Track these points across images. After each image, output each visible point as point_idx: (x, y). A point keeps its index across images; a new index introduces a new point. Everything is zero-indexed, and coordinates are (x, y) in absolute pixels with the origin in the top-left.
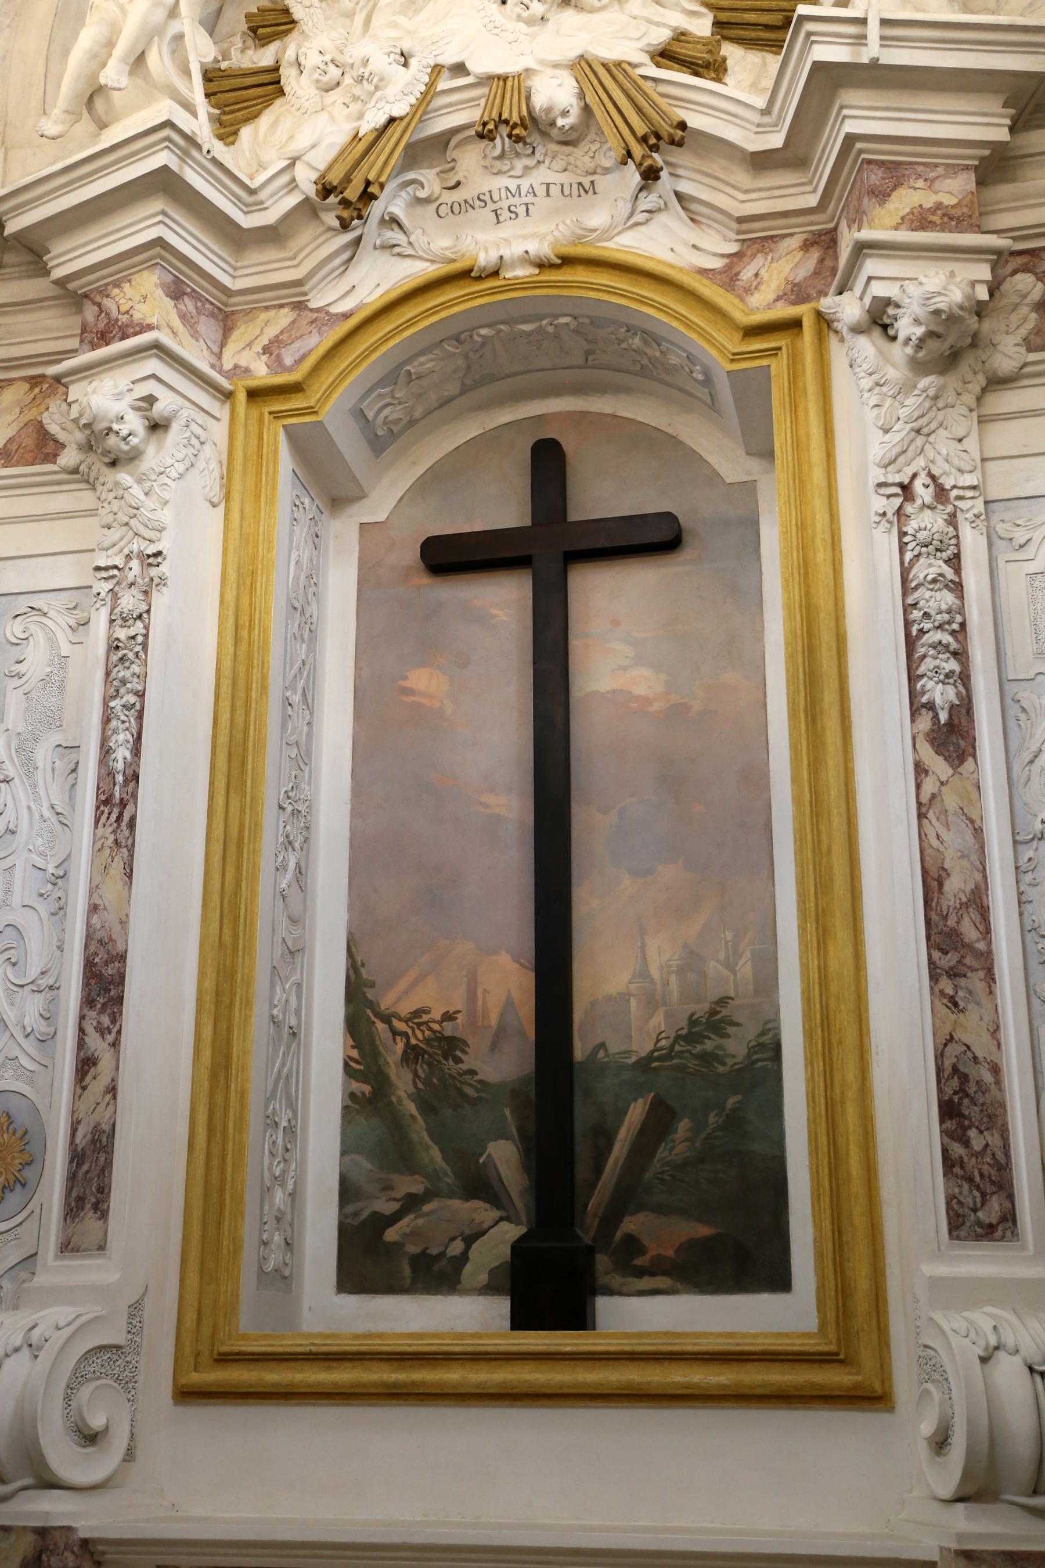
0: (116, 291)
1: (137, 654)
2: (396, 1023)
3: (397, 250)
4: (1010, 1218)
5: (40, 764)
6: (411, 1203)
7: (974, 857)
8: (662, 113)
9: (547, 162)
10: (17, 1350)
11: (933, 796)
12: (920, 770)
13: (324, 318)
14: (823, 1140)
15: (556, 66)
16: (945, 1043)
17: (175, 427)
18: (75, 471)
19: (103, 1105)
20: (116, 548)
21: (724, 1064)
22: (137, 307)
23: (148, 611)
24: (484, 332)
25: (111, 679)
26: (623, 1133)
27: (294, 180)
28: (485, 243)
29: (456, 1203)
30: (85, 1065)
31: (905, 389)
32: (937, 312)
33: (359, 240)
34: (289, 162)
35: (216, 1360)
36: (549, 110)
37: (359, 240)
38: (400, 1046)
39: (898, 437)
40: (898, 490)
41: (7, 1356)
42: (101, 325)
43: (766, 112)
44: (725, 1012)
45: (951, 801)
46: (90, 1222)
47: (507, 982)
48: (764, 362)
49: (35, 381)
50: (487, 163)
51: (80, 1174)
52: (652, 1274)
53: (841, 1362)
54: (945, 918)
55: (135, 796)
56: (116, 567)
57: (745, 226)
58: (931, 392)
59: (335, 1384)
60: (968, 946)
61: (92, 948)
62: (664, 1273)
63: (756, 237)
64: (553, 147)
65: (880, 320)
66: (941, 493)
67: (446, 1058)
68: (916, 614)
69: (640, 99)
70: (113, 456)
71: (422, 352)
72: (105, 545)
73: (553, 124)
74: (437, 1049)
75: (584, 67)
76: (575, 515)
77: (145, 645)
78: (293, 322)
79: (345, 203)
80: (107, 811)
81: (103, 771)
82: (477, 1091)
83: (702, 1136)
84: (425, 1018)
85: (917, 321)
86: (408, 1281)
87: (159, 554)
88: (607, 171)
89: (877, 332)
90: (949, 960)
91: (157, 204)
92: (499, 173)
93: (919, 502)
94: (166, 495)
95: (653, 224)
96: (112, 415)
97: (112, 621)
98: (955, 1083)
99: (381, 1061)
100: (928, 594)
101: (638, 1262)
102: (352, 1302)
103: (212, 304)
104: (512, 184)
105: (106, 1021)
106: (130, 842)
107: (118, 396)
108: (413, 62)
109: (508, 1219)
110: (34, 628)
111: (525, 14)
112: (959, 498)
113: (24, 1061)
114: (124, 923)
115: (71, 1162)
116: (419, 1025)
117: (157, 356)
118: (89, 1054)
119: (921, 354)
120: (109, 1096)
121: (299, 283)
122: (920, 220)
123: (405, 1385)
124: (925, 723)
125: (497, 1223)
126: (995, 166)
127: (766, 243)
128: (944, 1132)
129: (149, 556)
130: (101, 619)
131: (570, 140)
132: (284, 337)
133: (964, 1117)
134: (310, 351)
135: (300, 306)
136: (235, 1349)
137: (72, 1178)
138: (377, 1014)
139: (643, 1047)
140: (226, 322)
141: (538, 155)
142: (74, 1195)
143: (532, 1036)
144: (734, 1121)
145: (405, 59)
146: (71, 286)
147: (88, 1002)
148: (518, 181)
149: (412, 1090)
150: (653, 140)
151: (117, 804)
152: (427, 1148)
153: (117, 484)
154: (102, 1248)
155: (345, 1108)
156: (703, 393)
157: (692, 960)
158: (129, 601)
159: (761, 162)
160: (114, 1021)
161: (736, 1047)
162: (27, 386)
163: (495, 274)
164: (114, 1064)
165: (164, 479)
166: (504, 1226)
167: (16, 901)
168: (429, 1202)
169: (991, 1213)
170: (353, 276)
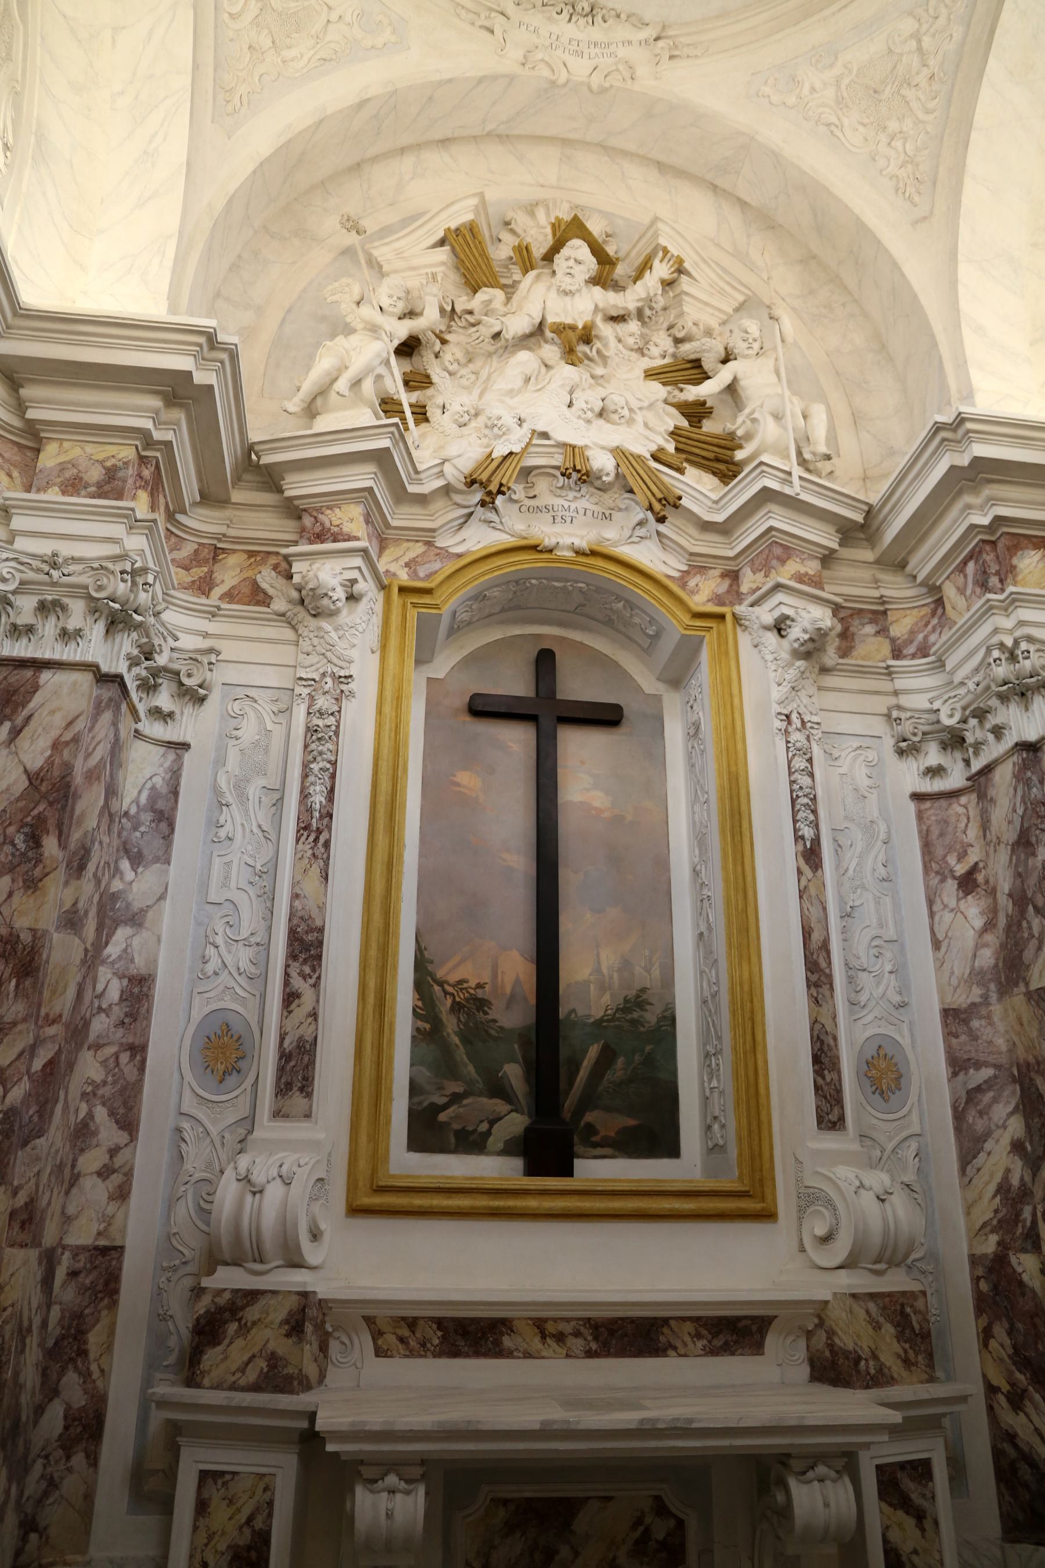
0: (328, 512)
1: (330, 738)
2: (447, 987)
3: (492, 524)
4: (842, 1118)
5: (251, 798)
6: (456, 1098)
7: (824, 922)
8: (667, 488)
9: (587, 497)
10: (274, 1179)
11: (805, 887)
12: (800, 872)
13: (444, 554)
14: (742, 1072)
15: (603, 448)
16: (814, 1022)
17: (365, 600)
18: (283, 615)
19: (306, 1025)
20: (313, 668)
21: (643, 1026)
22: (345, 524)
23: (339, 712)
24: (533, 581)
25: (309, 749)
26: (585, 1063)
27: (442, 471)
28: (546, 533)
29: (484, 1100)
30: (290, 998)
31: (790, 665)
32: (819, 629)
33: (472, 513)
35: (375, 1191)
36: (601, 470)
37: (472, 513)
38: (449, 1001)
39: (785, 690)
40: (784, 718)
41: (268, 1182)
42: (318, 529)
43: (716, 502)
44: (645, 997)
45: (813, 891)
46: (297, 1100)
47: (516, 969)
48: (703, 633)
49: (251, 554)
50: (553, 489)
51: (288, 1068)
52: (602, 1146)
53: (750, 1196)
54: (812, 954)
55: (329, 827)
56: (314, 680)
57: (693, 558)
58: (802, 669)
59: (459, 1207)
60: (822, 970)
61: (295, 922)
62: (609, 1146)
63: (697, 565)
65: (780, 627)
66: (803, 723)
67: (478, 1011)
68: (796, 787)
69: (654, 478)
70: (320, 610)
71: (496, 586)
72: (306, 665)
73: (599, 478)
74: (473, 1005)
75: (619, 453)
76: (559, 696)
77: (337, 733)
78: (425, 552)
79: (489, 493)
80: (306, 834)
81: (302, 808)
82: (498, 1032)
83: (632, 1067)
84: (465, 985)
85: (805, 631)
86: (453, 1146)
87: (351, 676)
88: (620, 510)
89: (775, 632)
90: (814, 978)
91: (372, 468)
92: (560, 496)
93: (794, 726)
94: (355, 642)
95: (642, 544)
96: (330, 586)
97: (309, 713)
98: (818, 1044)
99: (437, 1010)
100: (800, 777)
101: (594, 1139)
102: (416, 1157)
104: (566, 504)
105: (307, 970)
106: (325, 856)
107: (335, 576)
108: (524, 424)
109: (516, 1111)
110: (247, 709)
111: (583, 416)
112: (812, 728)
113: (238, 990)
114: (322, 908)
115: (280, 1058)
116: (461, 989)
117: (362, 557)
118: (294, 990)
119: (802, 648)
120: (310, 1019)
121: (433, 530)
122: (800, 578)
123: (504, 1208)
124: (801, 848)
125: (509, 1113)
126: (828, 559)
127: (702, 569)
128: (815, 1071)
129: (340, 677)
130: (300, 712)
131: (603, 489)
132: (419, 560)
133: (821, 1063)
134: (436, 572)
135: (429, 544)
136: (389, 1184)
137: (281, 1070)
138: (435, 981)
139: (598, 1013)
140: (383, 544)
142: (283, 1080)
143: (532, 1000)
144: (649, 1061)
145: (521, 421)
147: (292, 956)
149: (456, 1029)
150: (664, 501)
151: (315, 830)
152: (466, 1065)
153: (319, 628)
154: (308, 1116)
155: (413, 1037)
156: (645, 643)
157: (626, 965)
158: (323, 702)
159: (707, 526)
160: (314, 970)
161: (651, 1017)
162: (245, 556)
164: (314, 999)
165: (353, 631)
166: (514, 1115)
167: (233, 885)
168: (467, 1098)
169: (833, 1117)
170: (465, 533)
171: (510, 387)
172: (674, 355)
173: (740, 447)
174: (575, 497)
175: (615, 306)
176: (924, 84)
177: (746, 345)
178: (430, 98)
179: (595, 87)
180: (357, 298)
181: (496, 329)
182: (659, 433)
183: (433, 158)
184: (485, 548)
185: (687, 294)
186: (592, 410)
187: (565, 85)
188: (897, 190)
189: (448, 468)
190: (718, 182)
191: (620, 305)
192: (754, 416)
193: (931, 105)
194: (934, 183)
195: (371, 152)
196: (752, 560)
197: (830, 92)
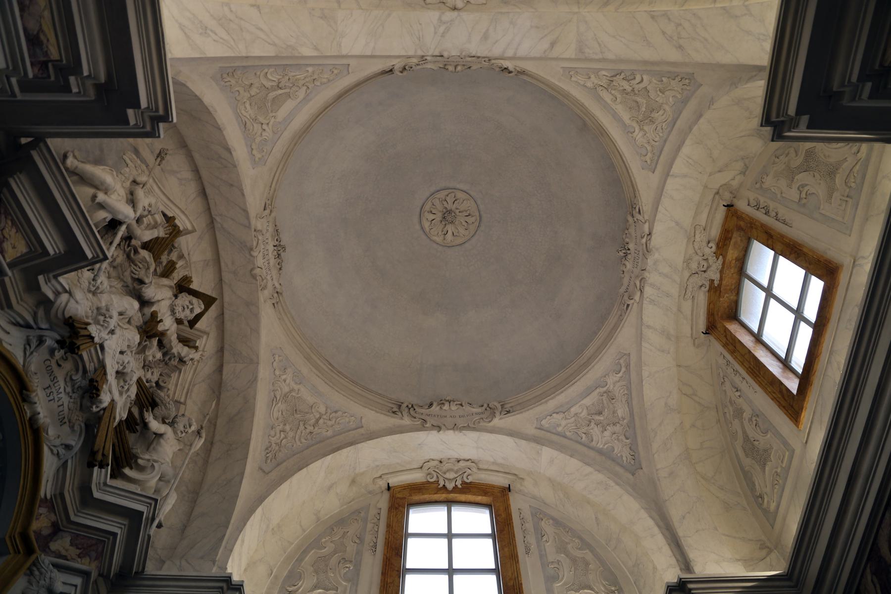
0: (10, 223)
3: (28, 347)
34: (67, 288)
63: (56, 503)
104: (62, 390)
121: (10, 306)
127: (52, 508)
141: (74, 395)
146: (5, 190)
163: (24, 400)
170: (13, 330)
172: (151, 387)
173: (131, 468)
175: (171, 341)
176: (308, 431)
177: (182, 429)
178: (232, 185)
179: (254, 272)
180: (139, 179)
181: (147, 281)
183: (192, 189)
184: (9, 351)
185: (180, 373)
187: (251, 255)
188: (267, 449)
189: (64, 297)
190: (226, 353)
192: (155, 464)
193: (303, 440)
194: (278, 465)
195: (196, 156)
196: (78, 535)
197: (286, 389)
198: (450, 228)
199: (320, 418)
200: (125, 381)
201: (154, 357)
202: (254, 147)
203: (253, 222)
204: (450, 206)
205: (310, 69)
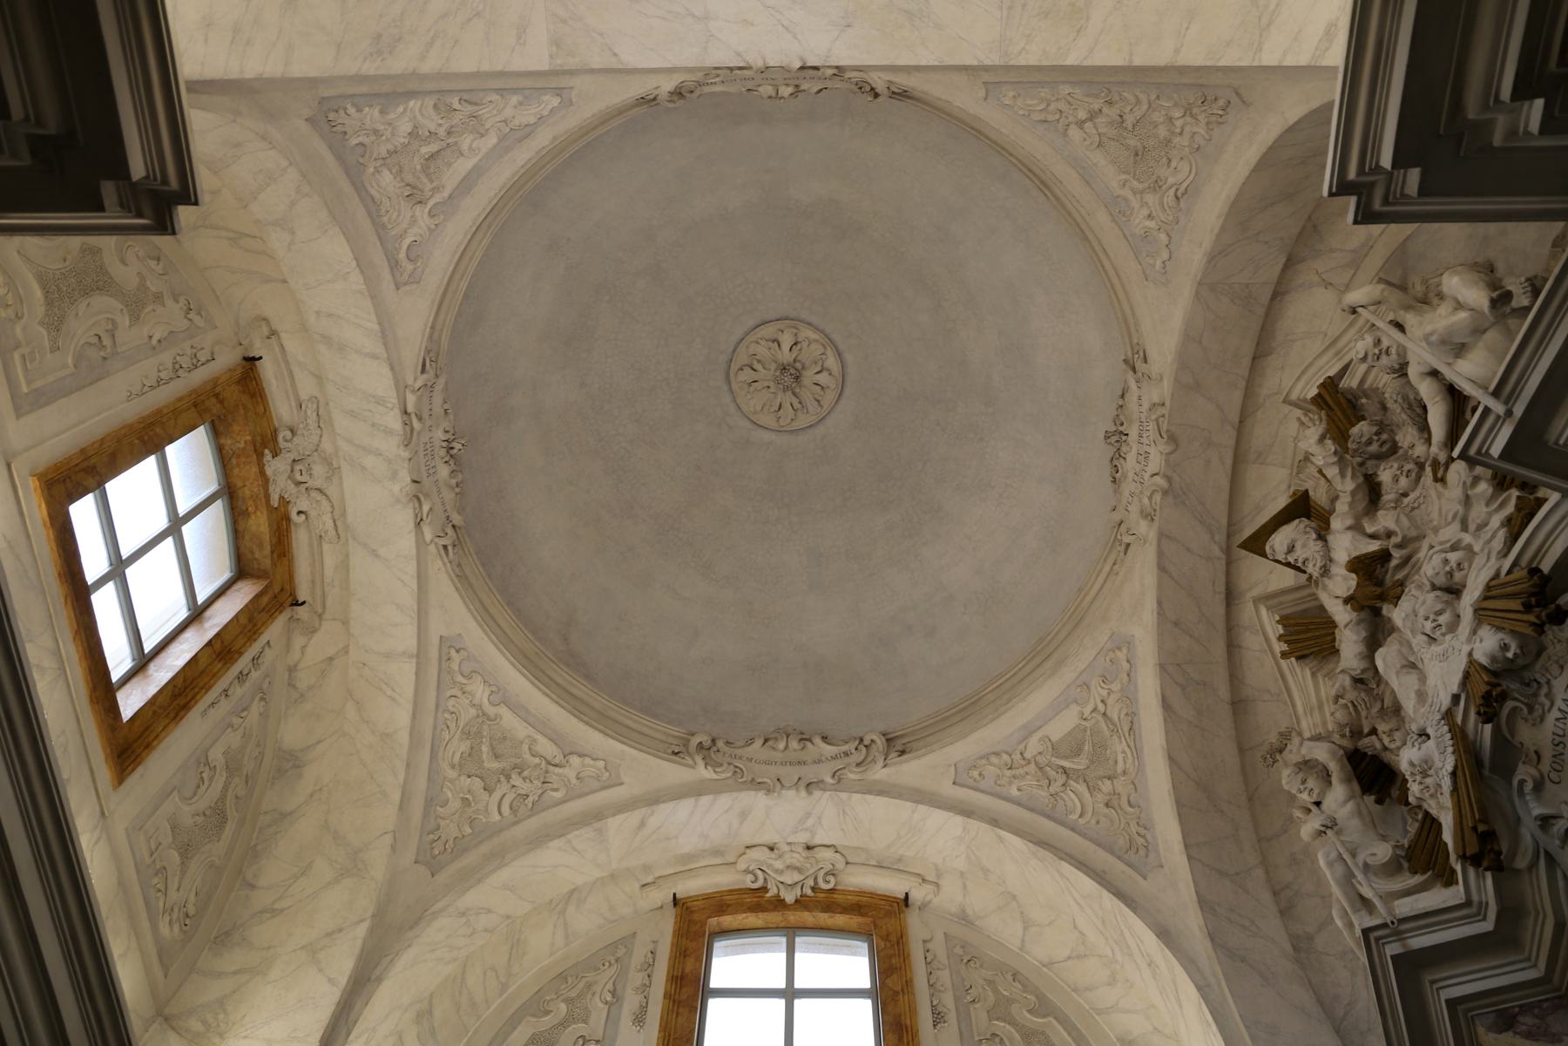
33: (1547, 854)
36: (1493, 659)
64: (1538, 666)
92: (1542, 719)
103: (1547, 1000)
104: (1555, 714)
108: (1429, 731)
111: (1444, 630)
141: (1543, 681)
148: (1555, 709)
171: (1413, 695)
174: (1547, 695)
178: (1176, 624)
182: (1490, 514)
185: (1362, 381)
186: (1439, 613)
187: (1169, 479)
191: (1349, 499)
195: (1224, 692)
198: (786, 356)
199: (1084, 122)
200: (1450, 574)
201: (1396, 479)
202: (1126, 678)
203: (1152, 535)
204: (788, 398)
205: (1015, 792)
